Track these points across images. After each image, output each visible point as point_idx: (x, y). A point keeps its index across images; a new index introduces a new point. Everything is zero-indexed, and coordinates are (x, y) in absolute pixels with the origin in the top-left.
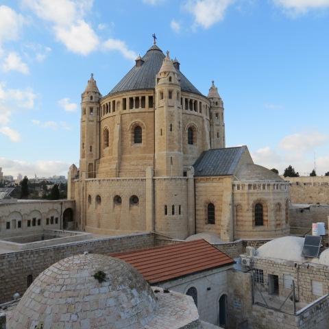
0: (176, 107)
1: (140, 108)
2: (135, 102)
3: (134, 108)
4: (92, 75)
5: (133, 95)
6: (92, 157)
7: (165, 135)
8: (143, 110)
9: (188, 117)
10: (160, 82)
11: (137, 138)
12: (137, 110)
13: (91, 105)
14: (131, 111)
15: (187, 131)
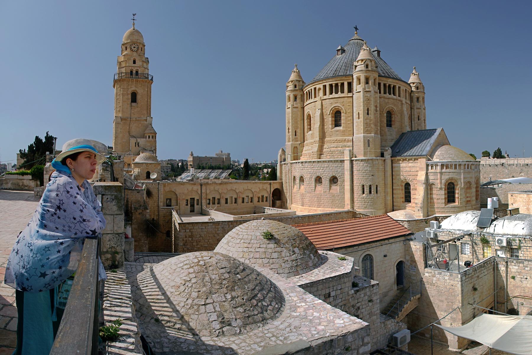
0: (373, 92)
1: (339, 93)
2: (335, 88)
3: (334, 93)
6: (297, 141)
7: (362, 119)
8: (343, 95)
9: (387, 101)
10: (358, 69)
11: (337, 123)
12: (336, 96)
14: (331, 96)
15: (385, 115)
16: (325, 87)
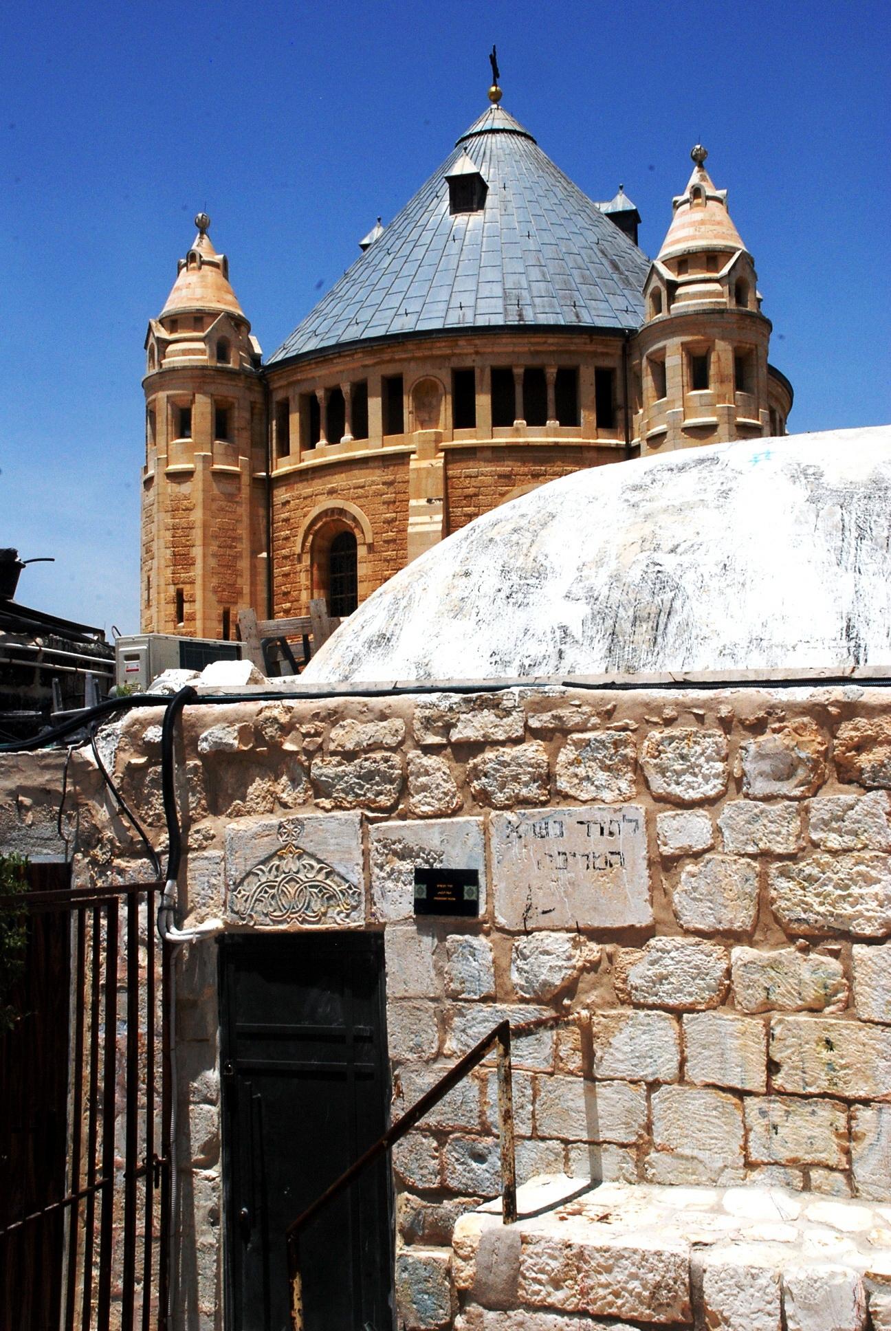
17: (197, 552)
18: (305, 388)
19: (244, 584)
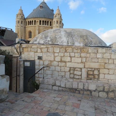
4: (21, 7)
5: (44, 20)
8: (48, 26)
13: (22, 20)
14: (43, 26)
16: (40, 21)
17: (20, 32)
18: (28, 21)
19: (23, 35)
